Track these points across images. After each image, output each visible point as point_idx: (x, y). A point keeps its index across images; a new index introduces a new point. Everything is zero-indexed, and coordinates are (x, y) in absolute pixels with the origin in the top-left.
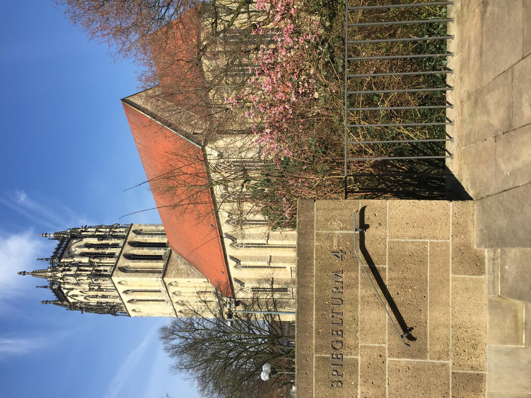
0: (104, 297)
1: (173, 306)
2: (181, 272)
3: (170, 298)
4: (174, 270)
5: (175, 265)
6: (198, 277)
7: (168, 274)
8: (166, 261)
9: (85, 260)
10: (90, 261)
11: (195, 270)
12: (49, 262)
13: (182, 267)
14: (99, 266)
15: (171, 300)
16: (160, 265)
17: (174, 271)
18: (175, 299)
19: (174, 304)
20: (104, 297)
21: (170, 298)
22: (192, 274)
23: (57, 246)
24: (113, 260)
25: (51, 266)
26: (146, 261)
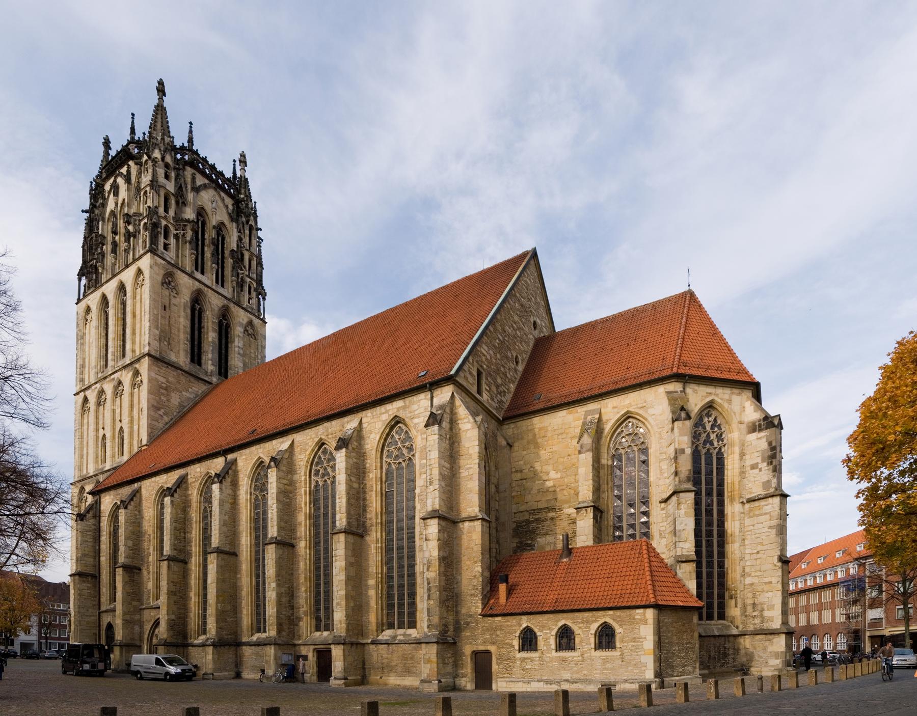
0: (115, 245)
1: (96, 383)
2: (163, 394)
3: (111, 375)
4: (168, 381)
5: (179, 386)
6: (151, 428)
7: (158, 367)
8: (186, 369)
9: (189, 214)
10: (188, 221)
11: (167, 423)
12: (186, 145)
13: (175, 399)
14: (176, 237)
15: (105, 378)
16: (181, 357)
17: (164, 380)
18: (108, 388)
19: (98, 385)
20: (115, 245)
21: (111, 375)
22: (157, 416)
23: (219, 168)
24: (188, 265)
25: (178, 147)
26: (189, 330)
